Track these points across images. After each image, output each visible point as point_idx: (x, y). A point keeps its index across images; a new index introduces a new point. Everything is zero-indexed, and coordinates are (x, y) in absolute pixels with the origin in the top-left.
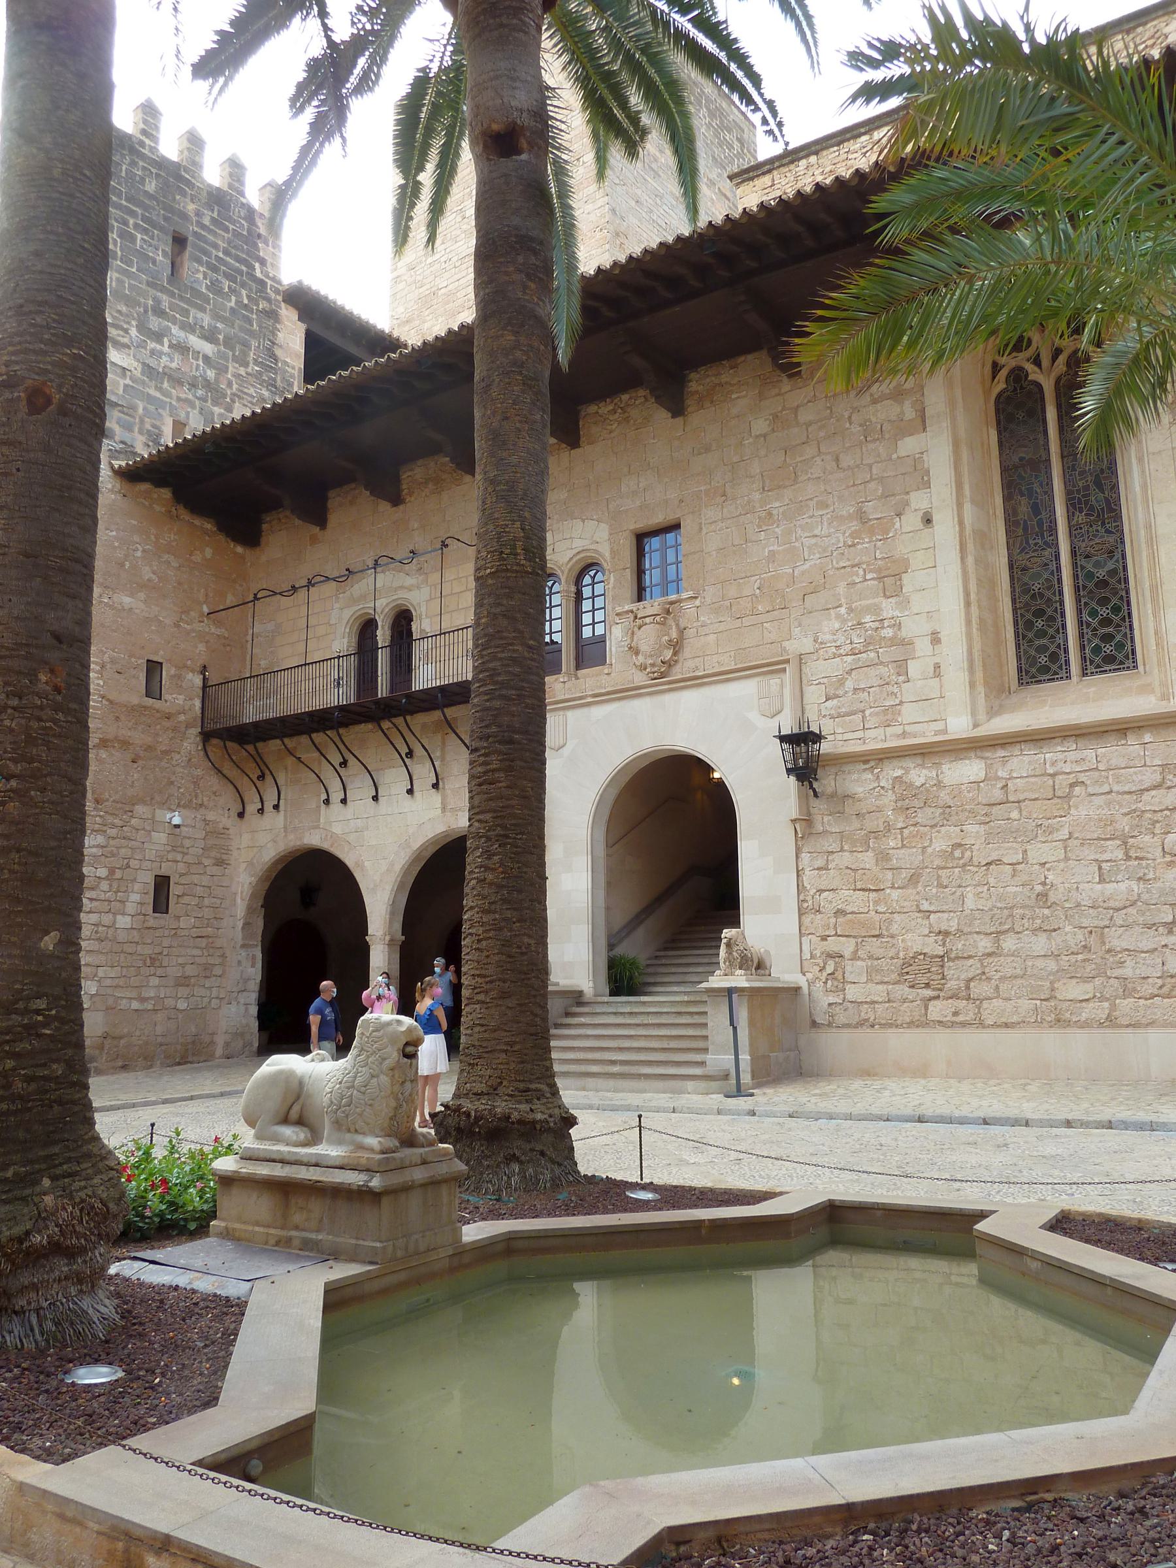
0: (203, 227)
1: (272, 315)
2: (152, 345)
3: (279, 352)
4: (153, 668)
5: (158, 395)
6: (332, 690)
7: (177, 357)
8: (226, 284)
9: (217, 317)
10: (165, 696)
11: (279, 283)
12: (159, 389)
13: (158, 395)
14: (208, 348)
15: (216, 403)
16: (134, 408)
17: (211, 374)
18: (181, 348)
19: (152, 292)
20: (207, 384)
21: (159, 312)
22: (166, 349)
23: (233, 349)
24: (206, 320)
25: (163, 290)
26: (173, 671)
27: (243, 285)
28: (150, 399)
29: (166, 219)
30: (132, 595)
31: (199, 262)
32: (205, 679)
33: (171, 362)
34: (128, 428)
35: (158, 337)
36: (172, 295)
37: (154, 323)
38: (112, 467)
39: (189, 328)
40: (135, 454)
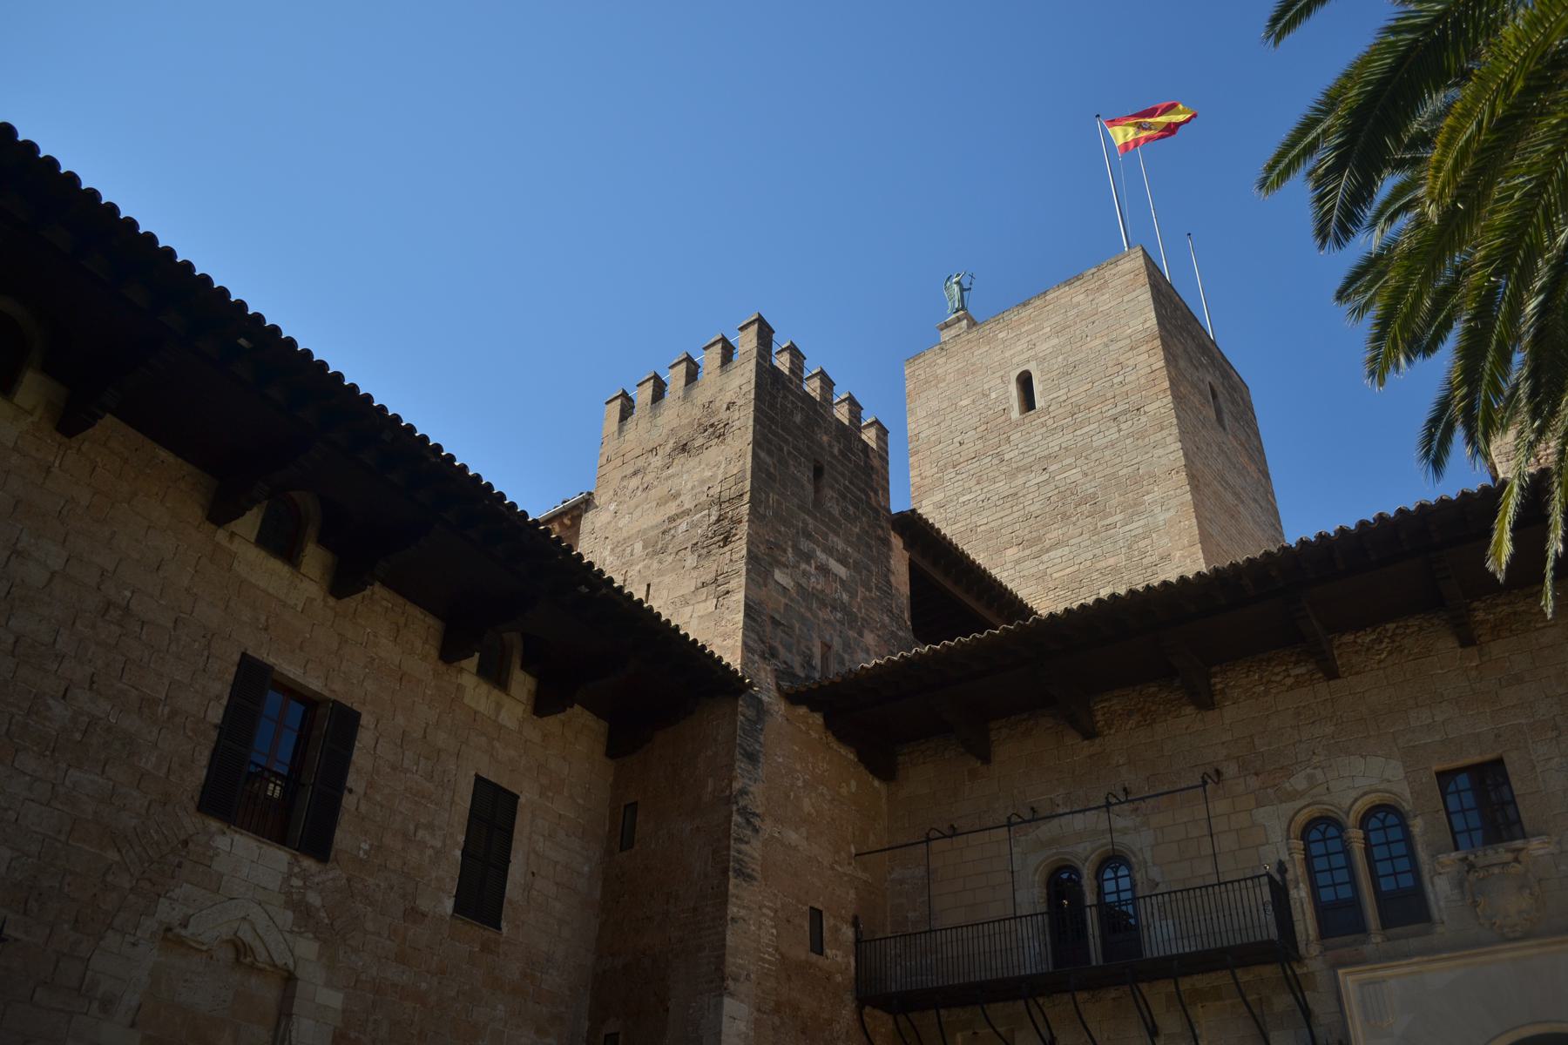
0: (834, 456)
1: (886, 542)
2: (803, 566)
3: (892, 579)
4: (816, 915)
5: (808, 615)
6: (1031, 952)
7: (822, 580)
8: (851, 510)
9: (848, 542)
10: (828, 952)
11: (889, 511)
12: (810, 609)
13: (808, 615)
14: (842, 571)
15: (851, 628)
16: (791, 627)
17: (845, 597)
18: (824, 570)
19: (803, 515)
20: (845, 609)
21: (808, 536)
22: (813, 571)
23: (860, 573)
24: (840, 545)
25: (809, 513)
26: (832, 922)
27: (864, 513)
28: (802, 618)
29: (809, 448)
30: (796, 830)
31: (832, 488)
32: (857, 932)
33: (816, 583)
34: (789, 648)
35: (808, 557)
36: (815, 518)
37: (805, 545)
38: (779, 688)
39: (830, 551)
40: (795, 675)
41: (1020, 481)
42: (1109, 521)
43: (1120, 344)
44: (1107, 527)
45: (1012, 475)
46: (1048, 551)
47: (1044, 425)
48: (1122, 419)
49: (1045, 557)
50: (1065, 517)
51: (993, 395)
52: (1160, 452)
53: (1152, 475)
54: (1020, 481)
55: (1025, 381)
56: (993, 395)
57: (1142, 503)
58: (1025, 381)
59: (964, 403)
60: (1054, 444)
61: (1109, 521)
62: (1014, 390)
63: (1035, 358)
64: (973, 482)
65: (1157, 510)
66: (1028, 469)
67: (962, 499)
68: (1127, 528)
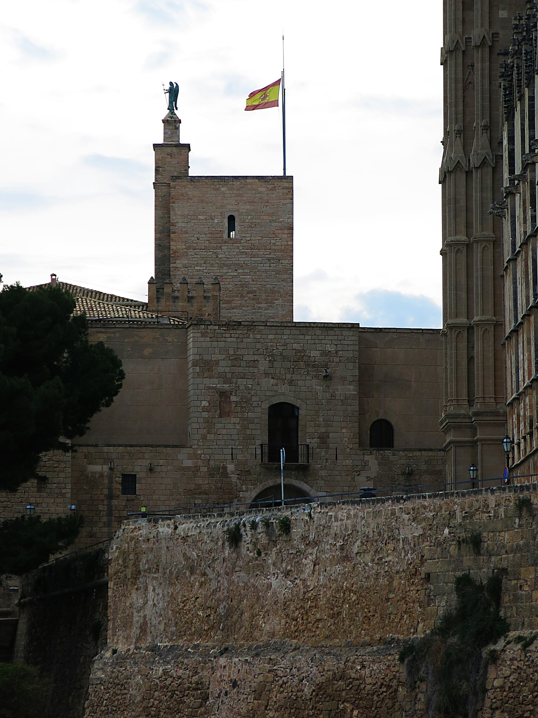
41: (225, 271)
42: (260, 305)
43: (277, 224)
44: (259, 308)
45: (221, 267)
46: (233, 309)
47: (238, 248)
48: (272, 261)
49: (232, 311)
50: (242, 296)
51: (216, 221)
52: (284, 284)
53: (279, 292)
54: (224, 270)
55: (231, 219)
56: (216, 221)
57: (274, 303)
58: (231, 219)
59: (201, 217)
60: (242, 259)
61: (260, 305)
62: (226, 221)
63: (238, 210)
64: (202, 262)
65: (280, 308)
66: (228, 266)
67: (196, 268)
68: (267, 311)
